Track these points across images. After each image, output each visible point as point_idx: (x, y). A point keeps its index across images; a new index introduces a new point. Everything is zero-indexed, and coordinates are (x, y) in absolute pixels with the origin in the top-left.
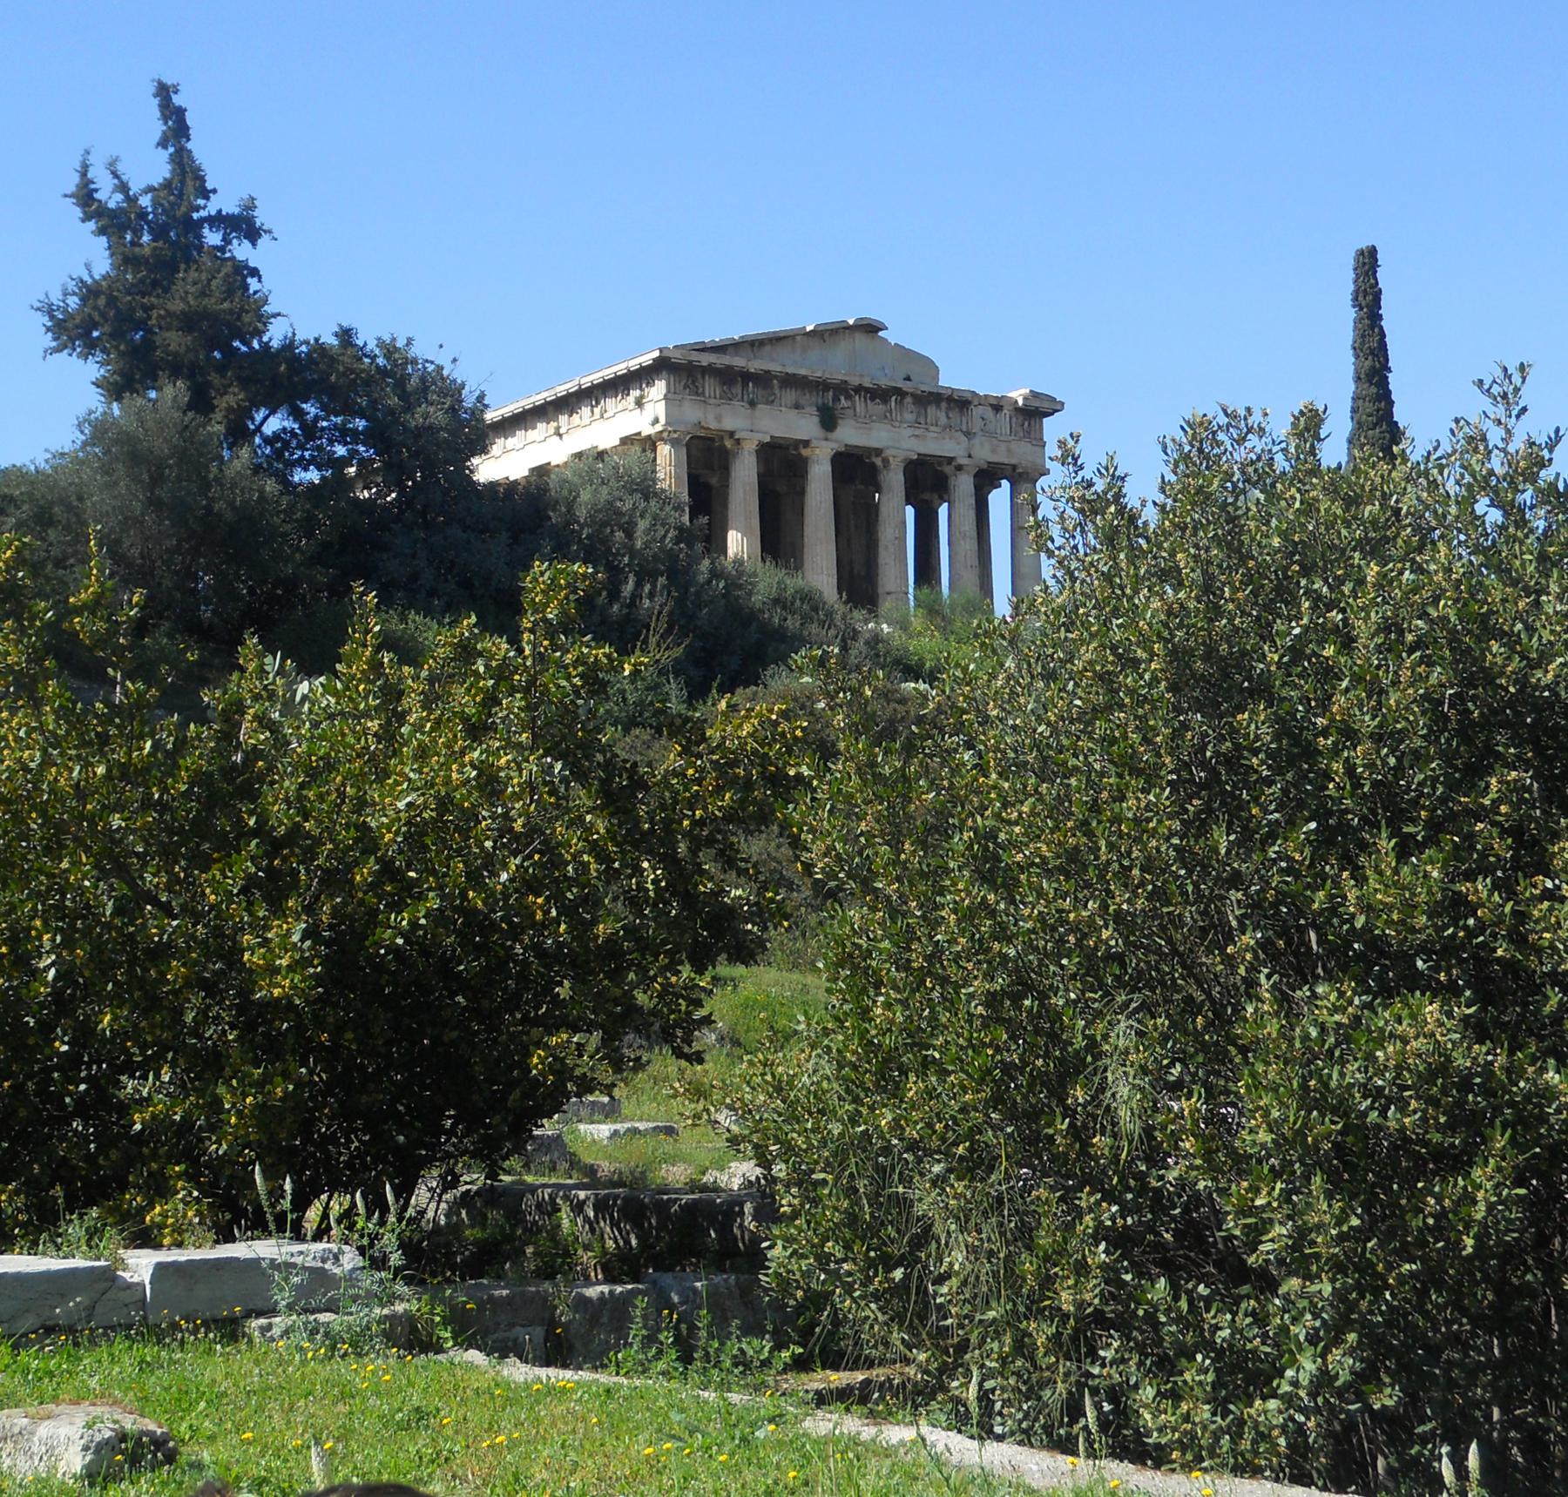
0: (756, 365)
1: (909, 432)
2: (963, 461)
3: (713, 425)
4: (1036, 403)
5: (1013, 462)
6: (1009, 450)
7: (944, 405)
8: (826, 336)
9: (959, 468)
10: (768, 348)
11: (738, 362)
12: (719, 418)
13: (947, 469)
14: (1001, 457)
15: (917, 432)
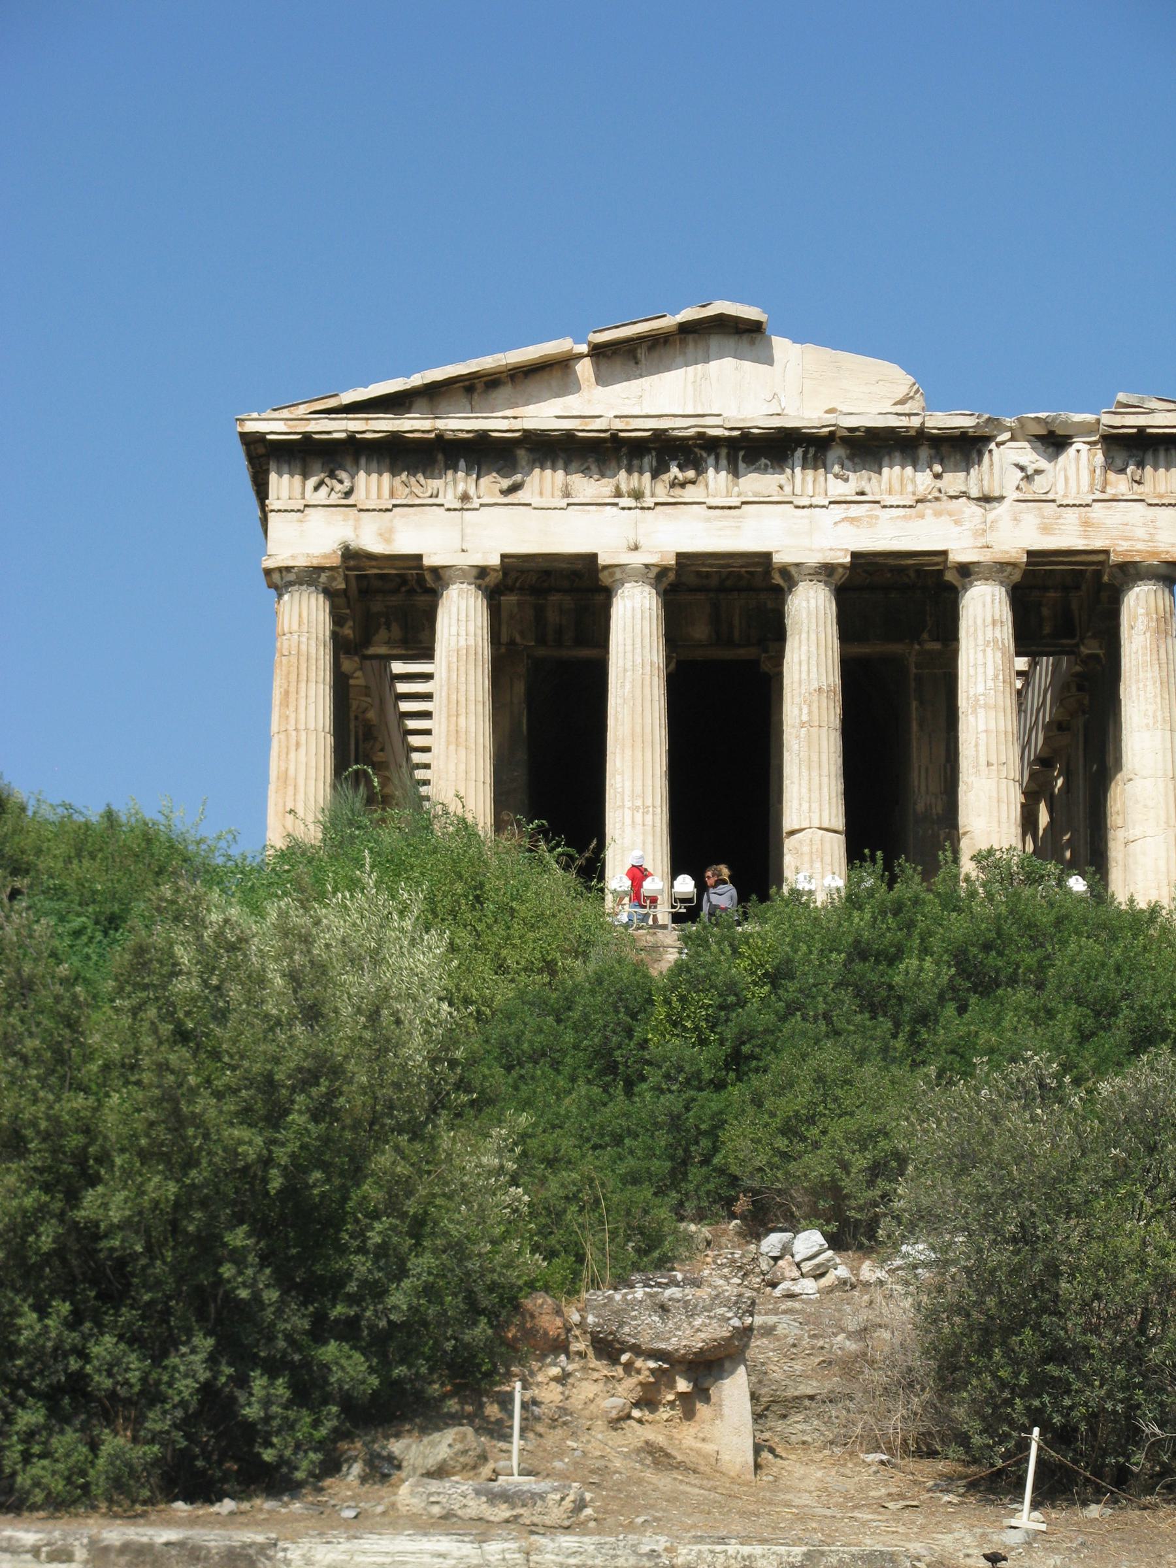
0: (459, 423)
1: (838, 511)
2: (957, 557)
3: (375, 546)
4: (1141, 421)
5: (1097, 544)
6: (1086, 523)
7: (924, 453)
8: (641, 353)
9: (966, 571)
10: (505, 392)
11: (414, 424)
12: (386, 535)
13: (950, 576)
14: (1068, 536)
15: (855, 511)
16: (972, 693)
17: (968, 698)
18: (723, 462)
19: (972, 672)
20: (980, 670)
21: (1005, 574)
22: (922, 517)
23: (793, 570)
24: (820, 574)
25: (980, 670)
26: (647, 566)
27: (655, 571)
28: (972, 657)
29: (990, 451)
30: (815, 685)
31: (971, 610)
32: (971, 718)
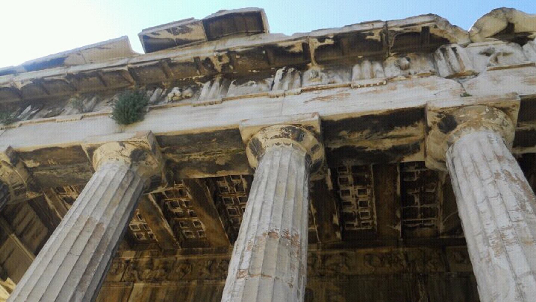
16: (490, 230)
17: (486, 238)
18: (216, 84)
19: (483, 207)
20: (496, 202)
21: (497, 121)
22: (395, 89)
23: (260, 136)
24: (287, 136)
25: (496, 202)
26: (122, 143)
27: (130, 148)
28: (479, 195)
29: (454, 49)
30: (266, 229)
31: (465, 155)
32: (500, 262)
